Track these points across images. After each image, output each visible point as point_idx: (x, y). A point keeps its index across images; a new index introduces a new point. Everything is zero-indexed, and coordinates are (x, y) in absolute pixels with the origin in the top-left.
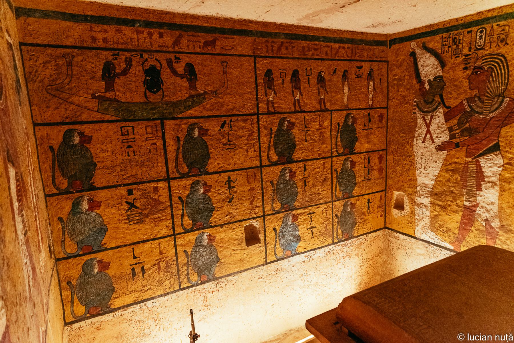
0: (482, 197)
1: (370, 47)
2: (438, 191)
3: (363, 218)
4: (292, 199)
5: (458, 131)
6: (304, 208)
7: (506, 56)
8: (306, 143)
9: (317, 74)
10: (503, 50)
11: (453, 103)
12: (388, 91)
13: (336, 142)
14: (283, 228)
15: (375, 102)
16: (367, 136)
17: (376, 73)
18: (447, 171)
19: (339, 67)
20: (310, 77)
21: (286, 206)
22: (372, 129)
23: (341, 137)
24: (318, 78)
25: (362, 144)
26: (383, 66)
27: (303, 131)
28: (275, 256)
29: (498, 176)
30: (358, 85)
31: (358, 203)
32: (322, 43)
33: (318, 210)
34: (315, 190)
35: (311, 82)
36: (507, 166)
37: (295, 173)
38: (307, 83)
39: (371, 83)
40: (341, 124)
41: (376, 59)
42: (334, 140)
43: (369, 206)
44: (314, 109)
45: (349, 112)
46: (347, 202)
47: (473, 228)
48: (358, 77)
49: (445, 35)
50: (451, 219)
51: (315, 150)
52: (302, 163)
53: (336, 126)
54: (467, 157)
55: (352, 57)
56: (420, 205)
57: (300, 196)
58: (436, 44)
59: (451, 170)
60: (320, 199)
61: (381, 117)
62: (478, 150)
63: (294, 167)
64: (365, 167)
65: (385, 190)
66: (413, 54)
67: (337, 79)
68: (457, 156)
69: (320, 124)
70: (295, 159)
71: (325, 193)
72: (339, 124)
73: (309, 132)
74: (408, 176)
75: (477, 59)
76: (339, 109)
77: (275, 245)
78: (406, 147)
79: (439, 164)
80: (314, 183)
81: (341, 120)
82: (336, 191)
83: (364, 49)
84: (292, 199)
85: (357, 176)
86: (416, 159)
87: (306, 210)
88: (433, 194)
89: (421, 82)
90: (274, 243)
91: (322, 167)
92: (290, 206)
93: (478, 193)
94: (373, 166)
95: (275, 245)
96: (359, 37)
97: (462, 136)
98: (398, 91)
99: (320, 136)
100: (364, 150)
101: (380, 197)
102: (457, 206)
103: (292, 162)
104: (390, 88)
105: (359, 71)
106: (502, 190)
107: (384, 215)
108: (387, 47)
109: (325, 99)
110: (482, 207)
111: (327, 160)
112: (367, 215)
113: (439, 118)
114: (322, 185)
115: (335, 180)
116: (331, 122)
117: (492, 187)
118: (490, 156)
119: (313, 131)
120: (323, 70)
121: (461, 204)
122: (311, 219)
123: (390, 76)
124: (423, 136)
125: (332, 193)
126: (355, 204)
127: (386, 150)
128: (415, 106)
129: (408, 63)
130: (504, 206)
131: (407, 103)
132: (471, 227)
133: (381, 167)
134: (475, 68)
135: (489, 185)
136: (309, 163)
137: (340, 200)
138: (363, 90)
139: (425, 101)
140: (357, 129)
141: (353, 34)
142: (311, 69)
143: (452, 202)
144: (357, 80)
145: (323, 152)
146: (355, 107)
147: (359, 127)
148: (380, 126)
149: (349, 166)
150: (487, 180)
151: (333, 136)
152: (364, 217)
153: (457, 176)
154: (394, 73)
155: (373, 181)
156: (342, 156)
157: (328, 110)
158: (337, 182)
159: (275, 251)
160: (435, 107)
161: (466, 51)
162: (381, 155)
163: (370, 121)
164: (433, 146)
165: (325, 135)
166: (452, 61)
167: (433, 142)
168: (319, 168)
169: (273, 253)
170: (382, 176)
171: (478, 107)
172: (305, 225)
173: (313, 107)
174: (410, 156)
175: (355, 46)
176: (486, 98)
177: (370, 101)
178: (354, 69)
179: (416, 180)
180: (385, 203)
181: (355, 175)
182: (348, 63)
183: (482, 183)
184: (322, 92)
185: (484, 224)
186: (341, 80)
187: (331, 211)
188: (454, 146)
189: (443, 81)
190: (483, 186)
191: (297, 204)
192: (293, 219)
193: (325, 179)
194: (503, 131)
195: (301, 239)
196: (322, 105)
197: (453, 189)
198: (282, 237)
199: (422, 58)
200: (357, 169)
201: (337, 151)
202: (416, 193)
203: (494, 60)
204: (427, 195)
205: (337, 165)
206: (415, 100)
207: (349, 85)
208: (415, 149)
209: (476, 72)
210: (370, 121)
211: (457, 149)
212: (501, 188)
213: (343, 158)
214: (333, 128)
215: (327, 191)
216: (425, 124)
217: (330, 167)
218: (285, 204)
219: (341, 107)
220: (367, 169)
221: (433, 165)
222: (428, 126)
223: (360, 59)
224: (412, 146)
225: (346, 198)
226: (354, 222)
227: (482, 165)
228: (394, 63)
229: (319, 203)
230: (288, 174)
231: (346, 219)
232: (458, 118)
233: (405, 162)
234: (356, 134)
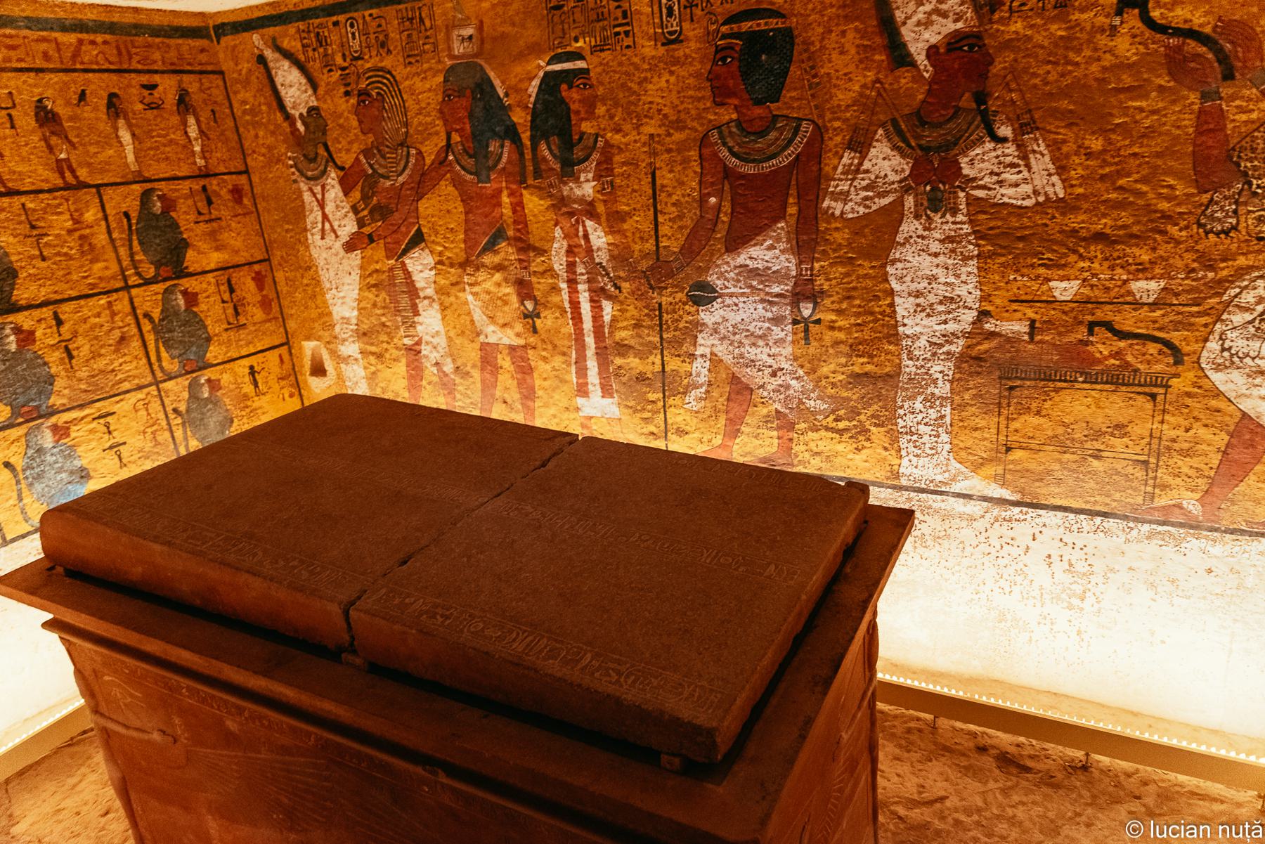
0: (424, 326)
1: (167, 41)
2: (366, 327)
3: (247, 407)
4: (40, 393)
5: (365, 213)
6: (81, 407)
7: (394, 73)
8: (44, 264)
9: (33, 105)
10: (387, 63)
11: (346, 159)
12: (239, 135)
13: (132, 255)
14: (33, 459)
15: (213, 162)
16: (213, 235)
17: (196, 98)
18: (370, 287)
19: (93, 87)
20: (13, 112)
21: (26, 409)
22: (220, 219)
23: (141, 243)
24: (37, 115)
25: (205, 253)
26: (211, 82)
27: (26, 236)
28: (27, 521)
29: (433, 285)
30: (156, 125)
31: (226, 379)
32: (25, 32)
33: (124, 406)
34: (101, 364)
35: (18, 123)
36: (439, 267)
37: (32, 333)
38: (8, 125)
39: (191, 120)
40: (134, 215)
41: (189, 68)
42: (123, 252)
43: (255, 380)
44: (46, 186)
45: (148, 186)
46: (196, 379)
47: (424, 383)
48: (152, 108)
49: (302, 25)
50: (394, 374)
51: (75, 277)
52: (45, 309)
53: (120, 219)
54: (388, 258)
55: (121, 63)
56: (346, 360)
57: (59, 384)
58: (293, 44)
59: (375, 286)
60: (121, 381)
61: (237, 193)
62: (398, 243)
63: (24, 320)
64: (223, 302)
65: (287, 343)
66: (261, 60)
67: (95, 111)
68: (376, 258)
69: (73, 219)
70: (23, 302)
71: (131, 366)
72: (126, 215)
73: (46, 239)
74: (317, 307)
75: (359, 77)
76: (118, 180)
77: (20, 499)
78: (299, 251)
79: (355, 276)
80: (93, 349)
81: (133, 206)
82: (159, 359)
83: (149, 46)
84: (40, 393)
85: (208, 322)
86: (320, 272)
87: (87, 411)
88: (363, 335)
89: (288, 117)
90: (15, 495)
91: (107, 312)
92: (38, 407)
93: (416, 319)
94: (244, 298)
95: (20, 499)
96: (129, 19)
97: (374, 220)
98: (257, 136)
99: (81, 245)
100: (212, 266)
101: (278, 359)
102: (397, 348)
103: (16, 309)
104: (241, 130)
105: (151, 94)
106: (444, 308)
107: (297, 393)
108: (212, 41)
109: (73, 161)
110: (427, 343)
111: (115, 296)
112: (256, 398)
113: (334, 192)
114: (117, 351)
115: (150, 338)
116: (104, 209)
117: (430, 305)
118: (416, 253)
119: (57, 236)
120: (49, 93)
121: (400, 344)
122: (108, 428)
123: (236, 105)
124: (320, 226)
125: (150, 364)
126: (219, 380)
127: (268, 260)
128: (291, 167)
129: (258, 78)
130: (452, 334)
131: (278, 161)
132: (422, 380)
133: (263, 296)
135: (426, 302)
136: (67, 308)
137: (176, 377)
138: (173, 136)
139: (304, 156)
140: (182, 223)
141: (110, 11)
142: (10, 93)
143: (388, 343)
144: (150, 114)
145: (100, 278)
146: (162, 176)
147: (184, 217)
148: (240, 211)
149: (181, 302)
150: (422, 294)
151: (118, 243)
152: (249, 403)
153: (383, 295)
154: (240, 96)
155: (253, 329)
156: (157, 283)
157: (88, 186)
158: (157, 341)
159: (23, 511)
160: (322, 168)
161: (339, 60)
162: (258, 273)
163: (210, 202)
164: (338, 245)
165: (94, 241)
166: (325, 77)
167: (337, 237)
168: (98, 315)
169: (20, 518)
170: (271, 316)
171: (381, 165)
172: (93, 444)
173: (43, 181)
174: (309, 268)
175: (124, 38)
176: (387, 150)
177: (198, 160)
178: (134, 91)
179: (330, 314)
180: (294, 369)
181: (201, 320)
182: (114, 77)
183: (417, 301)
184: (57, 145)
185: (436, 372)
186: (105, 117)
187: (159, 402)
188: (366, 241)
189: (321, 116)
190: (420, 306)
191: (56, 401)
192: (54, 435)
193: (123, 339)
194: (422, 205)
195: (92, 474)
196: (68, 174)
197: (384, 319)
198: (33, 478)
199: (279, 68)
200: (203, 307)
201: (138, 274)
202: (335, 337)
203: (380, 79)
204: (352, 339)
205: (149, 304)
206: (289, 154)
207: (130, 126)
208: (315, 253)
209: (364, 102)
210: (210, 202)
211: (373, 245)
212: (441, 304)
213: (160, 288)
214: (113, 225)
215: (134, 364)
216: (316, 203)
217: (128, 309)
218: (23, 406)
219: (122, 177)
220: (231, 305)
221: (347, 279)
222: (322, 205)
223: (146, 68)
224: (307, 247)
225: (193, 372)
226: (225, 418)
227: (410, 269)
228: (235, 75)
229: (120, 391)
230: (12, 338)
231: (203, 414)
232: (359, 187)
233: (305, 281)
234: (181, 233)
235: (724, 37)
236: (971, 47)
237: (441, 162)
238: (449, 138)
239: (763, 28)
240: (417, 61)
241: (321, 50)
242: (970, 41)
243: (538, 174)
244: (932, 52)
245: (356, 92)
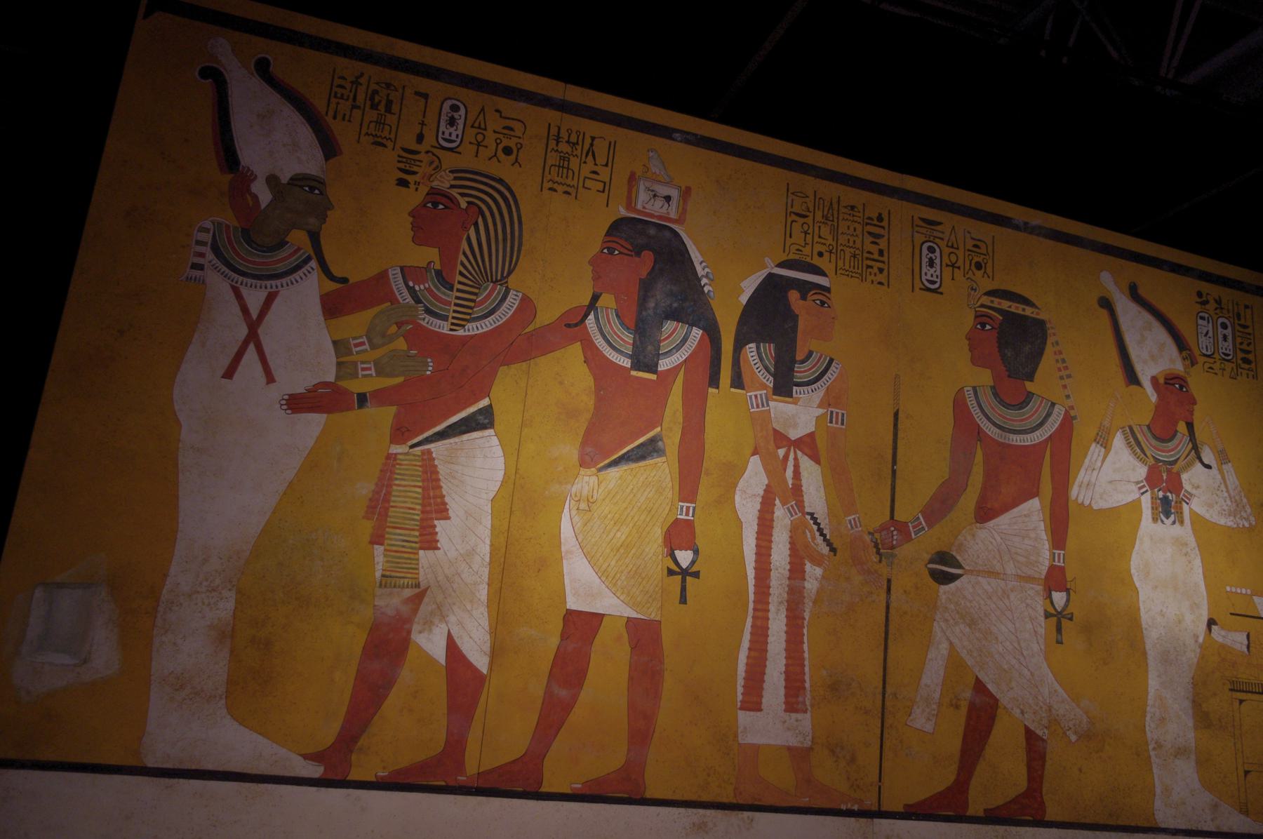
134: (433, 192)
235: (982, 306)
236: (1181, 387)
237: (573, 324)
238: (595, 298)
240: (567, 193)
241: (372, 115)
243: (738, 382)
245: (426, 190)
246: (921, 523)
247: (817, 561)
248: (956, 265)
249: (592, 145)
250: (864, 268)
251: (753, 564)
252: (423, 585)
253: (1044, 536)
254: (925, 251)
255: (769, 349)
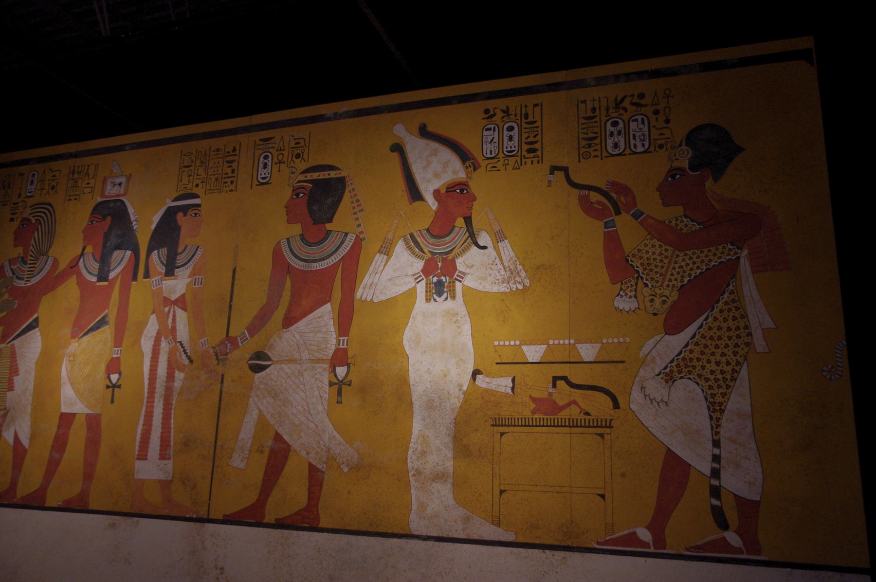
203: (42, 210)
236: (462, 191)
239: (327, 177)
240: (76, 199)
242: (464, 187)
244: (437, 194)
245: (19, 219)
246: (246, 336)
247: (181, 370)
248: (282, 161)
249: (88, 169)
250: (222, 183)
251: (148, 376)
252: (8, 409)
253: (332, 329)
254: (262, 159)
255: (164, 251)
